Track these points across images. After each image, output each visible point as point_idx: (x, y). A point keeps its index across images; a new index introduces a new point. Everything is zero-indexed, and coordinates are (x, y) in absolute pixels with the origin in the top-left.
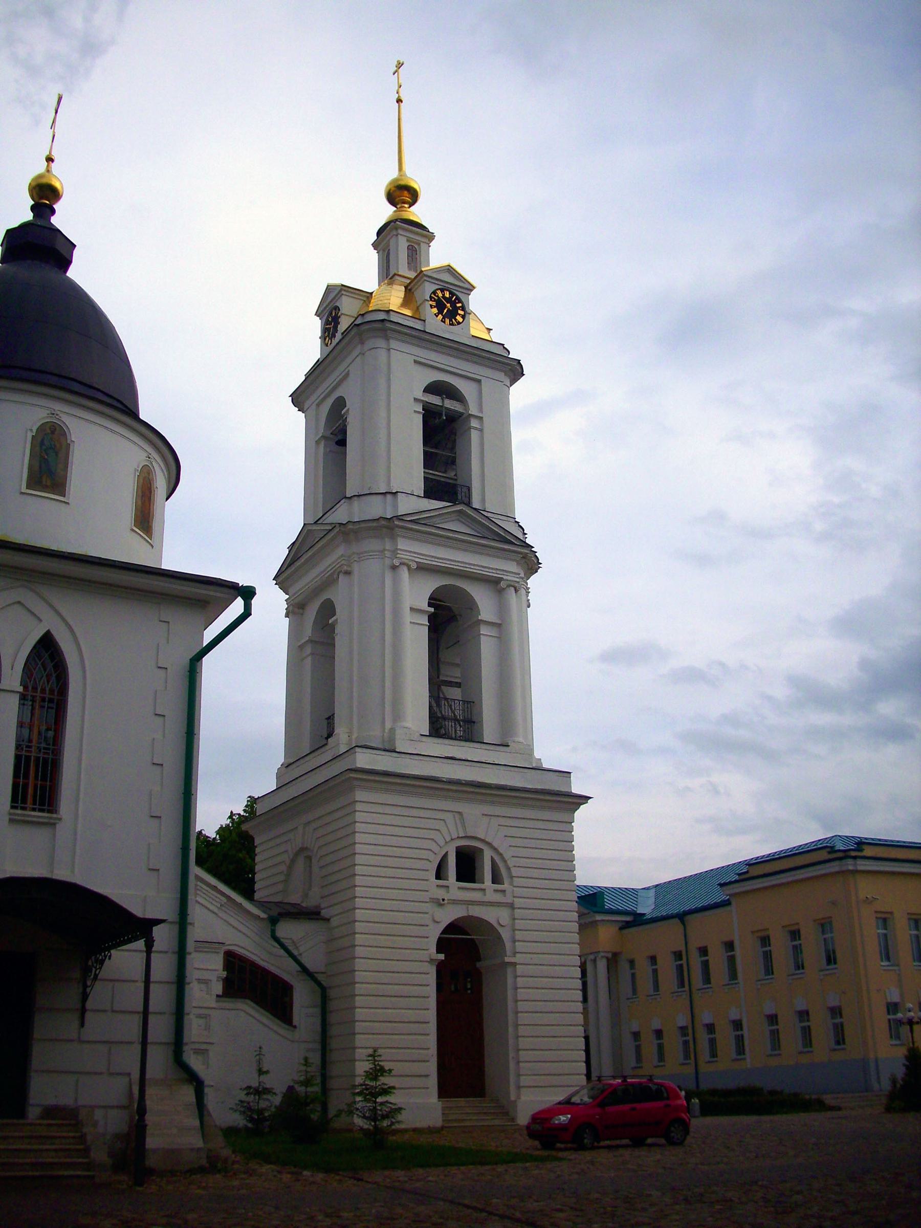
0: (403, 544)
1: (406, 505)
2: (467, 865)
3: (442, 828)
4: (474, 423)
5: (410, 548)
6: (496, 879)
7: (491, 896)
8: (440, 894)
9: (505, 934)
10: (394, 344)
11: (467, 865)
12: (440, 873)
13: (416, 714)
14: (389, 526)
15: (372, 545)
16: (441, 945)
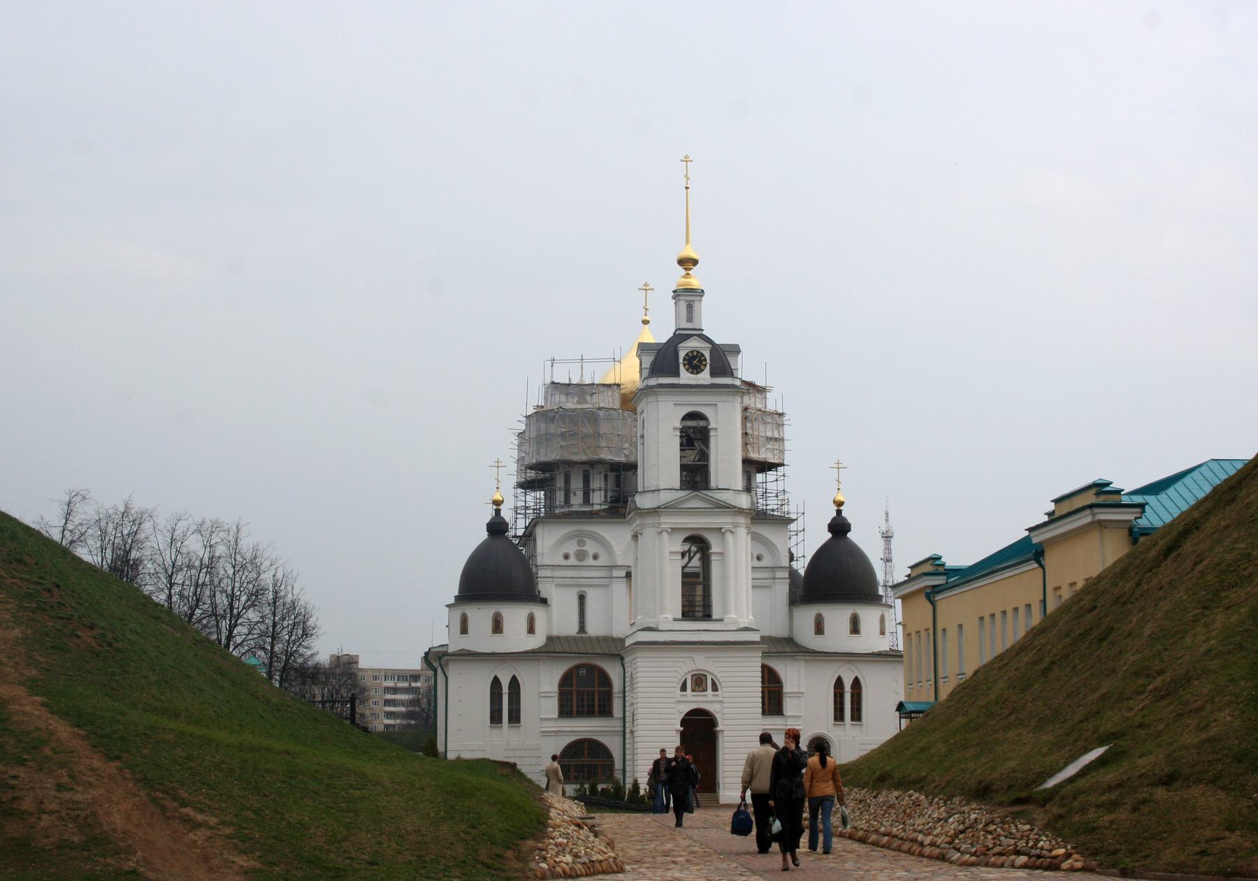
0: (664, 519)
1: (665, 498)
2: (699, 682)
3: (686, 665)
4: (712, 433)
5: (668, 521)
6: (715, 688)
7: (710, 698)
8: (684, 699)
9: (718, 717)
10: (660, 398)
11: (699, 682)
12: (684, 688)
13: (674, 604)
14: (655, 511)
15: (649, 520)
16: (683, 722)
